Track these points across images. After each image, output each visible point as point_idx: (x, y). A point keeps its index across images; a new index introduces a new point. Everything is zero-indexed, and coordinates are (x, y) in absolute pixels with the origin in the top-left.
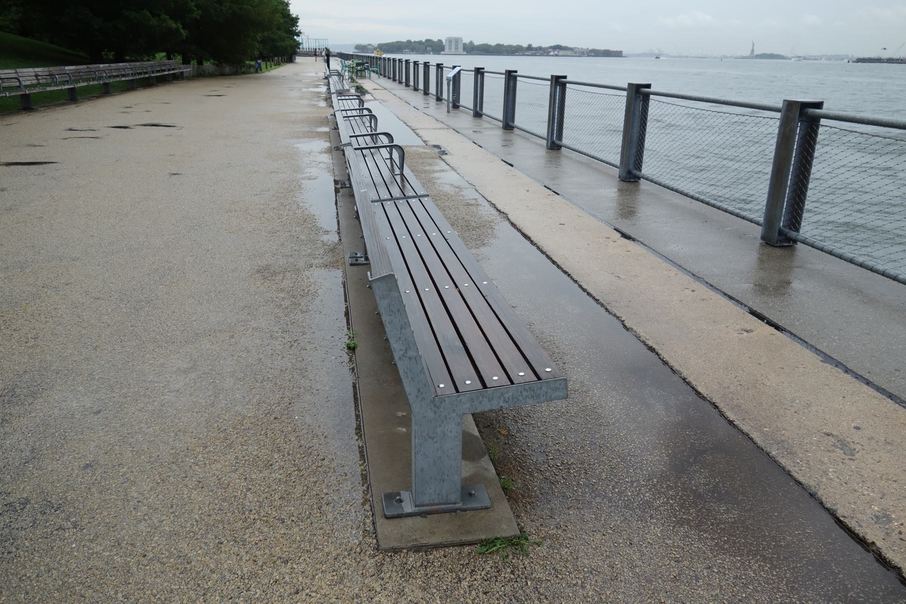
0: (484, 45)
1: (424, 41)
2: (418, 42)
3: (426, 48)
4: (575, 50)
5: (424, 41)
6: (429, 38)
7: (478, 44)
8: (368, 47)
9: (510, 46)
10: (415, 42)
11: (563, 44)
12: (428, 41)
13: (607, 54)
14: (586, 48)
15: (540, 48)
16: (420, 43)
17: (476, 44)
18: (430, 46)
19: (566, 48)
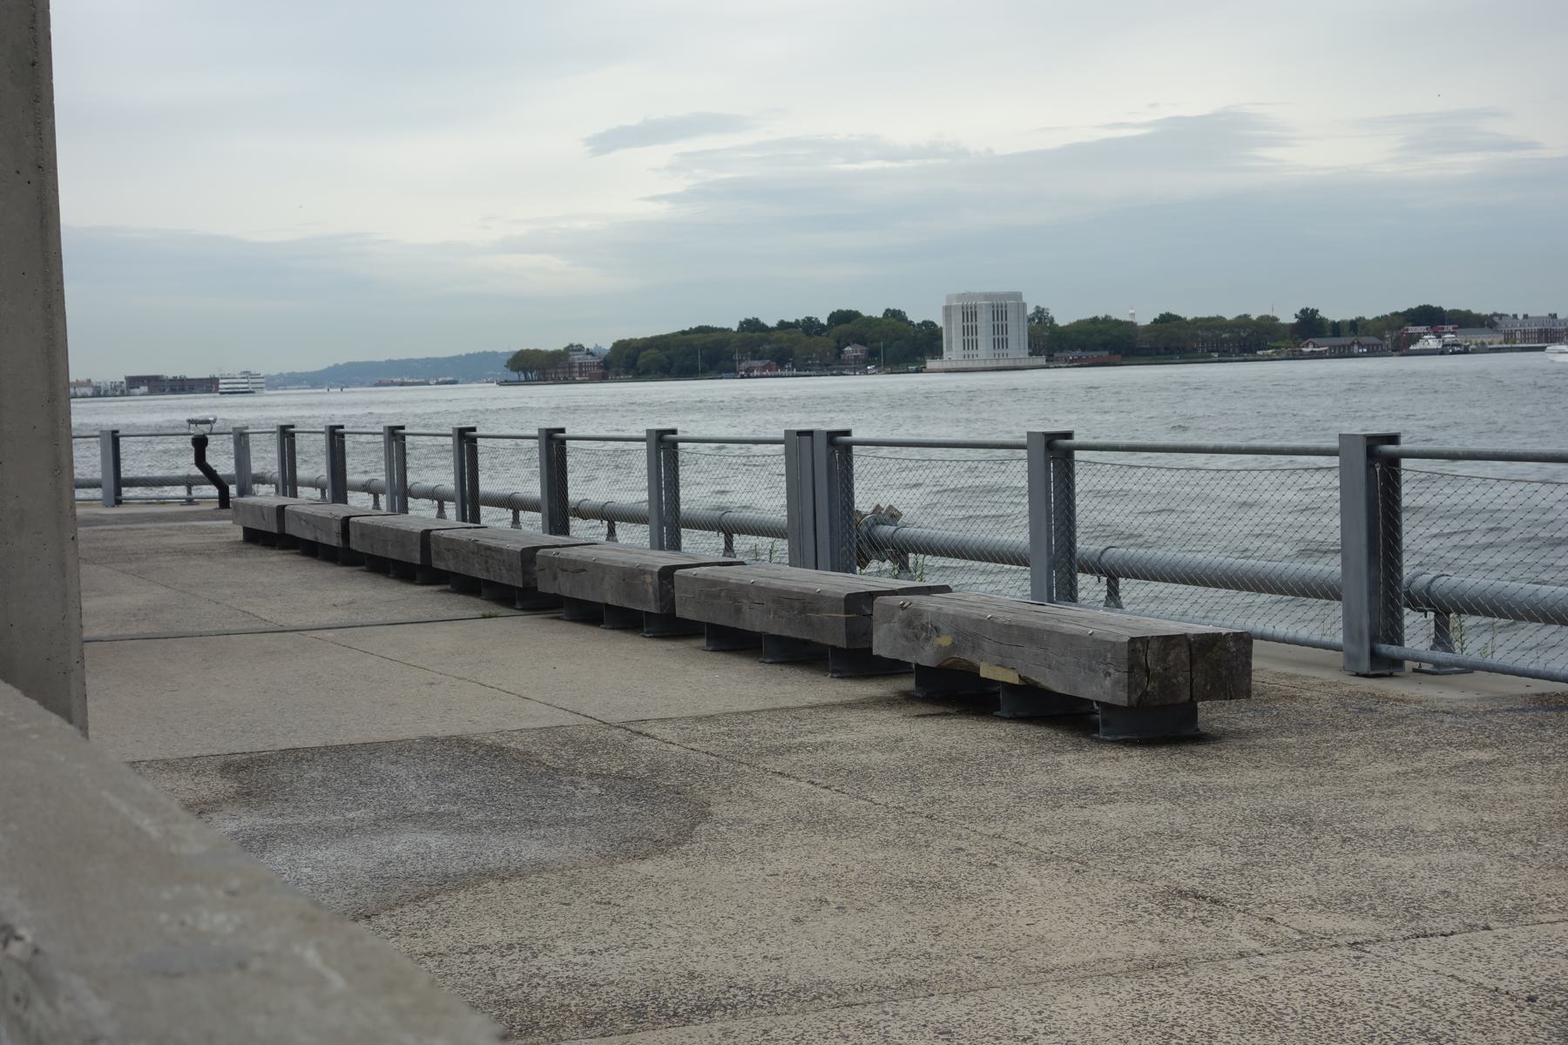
0: (1095, 320)
1: (824, 321)
2: (796, 324)
3: (840, 351)
4: (1504, 326)
5: (824, 321)
7: (1066, 324)
8: (577, 358)
9: (1213, 325)
10: (783, 325)
12: (840, 318)
14: (1544, 312)
15: (1356, 326)
16: (810, 326)
17: (1062, 320)
18: (860, 340)
19: (1465, 320)
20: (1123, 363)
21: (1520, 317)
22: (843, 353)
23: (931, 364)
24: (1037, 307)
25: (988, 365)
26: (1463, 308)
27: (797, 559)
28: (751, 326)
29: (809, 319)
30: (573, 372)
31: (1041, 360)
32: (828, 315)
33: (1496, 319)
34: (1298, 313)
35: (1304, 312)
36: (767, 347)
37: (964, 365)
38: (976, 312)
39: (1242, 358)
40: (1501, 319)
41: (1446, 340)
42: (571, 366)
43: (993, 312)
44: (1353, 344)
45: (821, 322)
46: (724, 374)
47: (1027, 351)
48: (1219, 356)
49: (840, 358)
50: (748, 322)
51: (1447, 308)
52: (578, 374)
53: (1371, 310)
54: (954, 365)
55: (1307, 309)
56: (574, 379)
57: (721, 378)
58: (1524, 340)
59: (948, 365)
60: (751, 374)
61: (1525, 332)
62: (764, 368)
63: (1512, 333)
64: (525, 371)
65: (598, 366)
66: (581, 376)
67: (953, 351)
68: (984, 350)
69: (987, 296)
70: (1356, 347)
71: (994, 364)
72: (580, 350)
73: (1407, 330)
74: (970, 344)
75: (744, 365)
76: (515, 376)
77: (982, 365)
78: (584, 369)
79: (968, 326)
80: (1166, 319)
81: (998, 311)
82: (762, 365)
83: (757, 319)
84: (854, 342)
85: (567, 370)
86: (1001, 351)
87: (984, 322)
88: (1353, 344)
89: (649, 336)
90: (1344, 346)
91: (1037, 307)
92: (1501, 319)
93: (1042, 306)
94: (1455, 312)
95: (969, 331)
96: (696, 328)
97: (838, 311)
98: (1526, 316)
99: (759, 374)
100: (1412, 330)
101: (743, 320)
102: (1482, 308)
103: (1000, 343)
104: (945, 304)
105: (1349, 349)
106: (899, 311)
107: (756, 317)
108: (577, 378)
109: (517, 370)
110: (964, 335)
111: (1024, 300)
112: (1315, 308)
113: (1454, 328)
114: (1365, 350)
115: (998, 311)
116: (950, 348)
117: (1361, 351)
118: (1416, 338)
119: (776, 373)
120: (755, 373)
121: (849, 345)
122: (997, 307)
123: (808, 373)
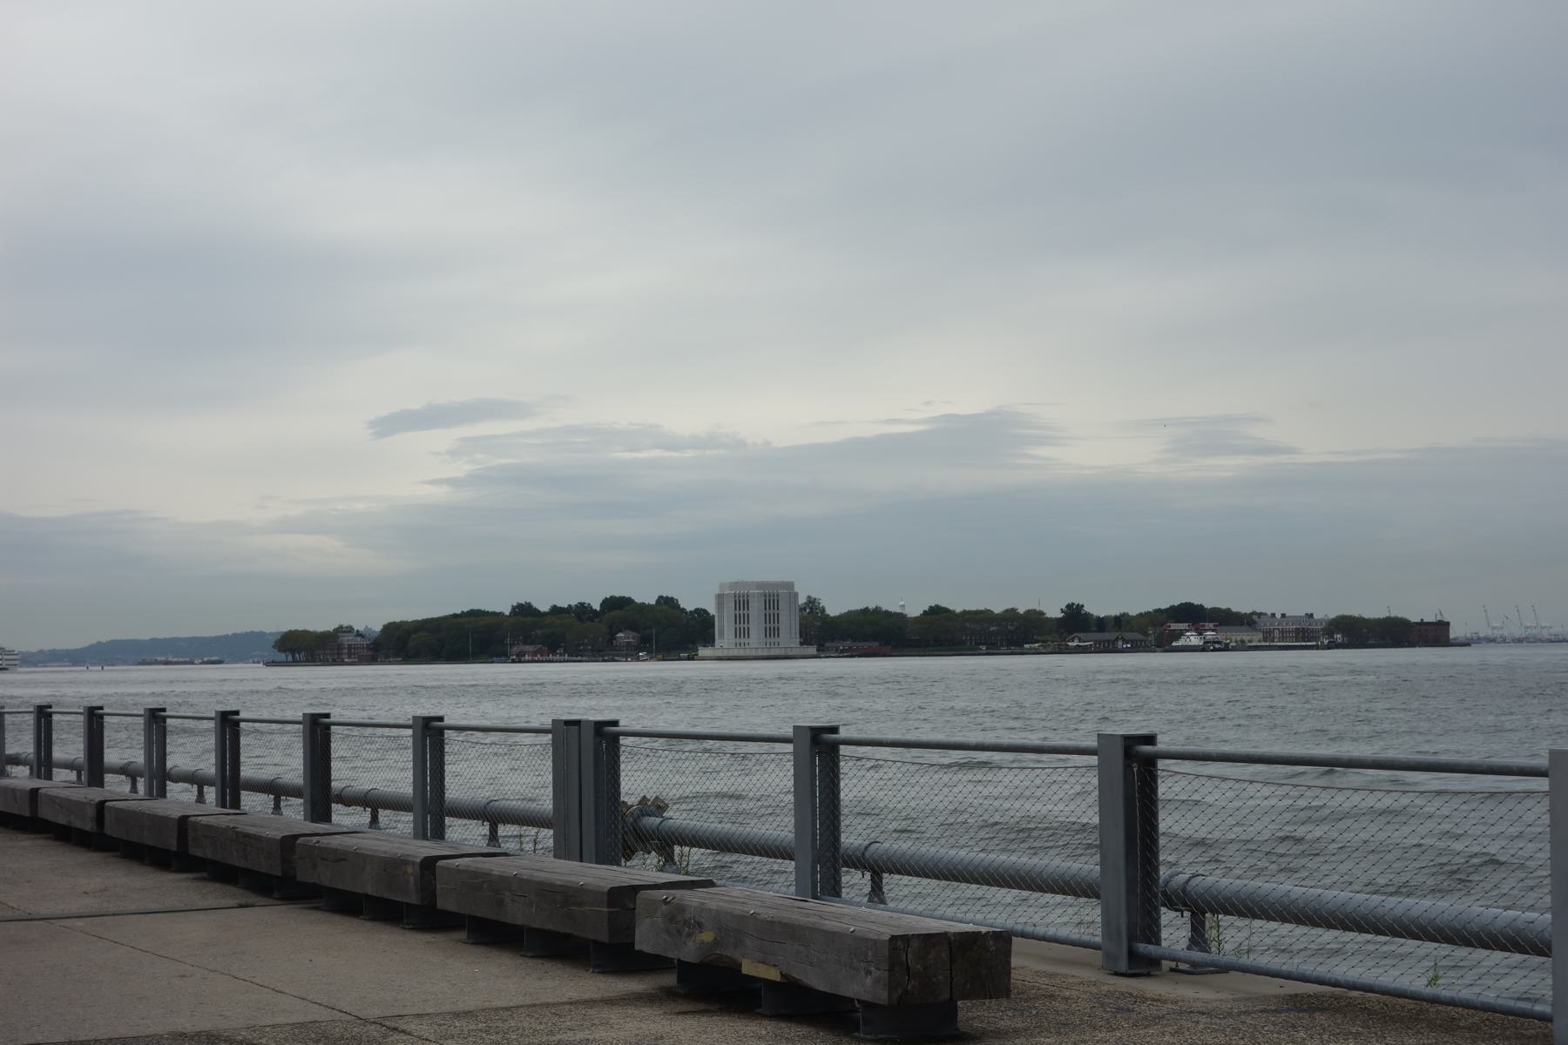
1: (597, 607)
3: (612, 637)
5: (597, 607)
6: (618, 593)
8: (346, 639)
9: (984, 617)
10: (555, 610)
11: (1208, 600)
12: (613, 604)
13: (1395, 633)
14: (1300, 612)
15: (1120, 622)
16: (582, 611)
18: (632, 627)
19: (1225, 618)
20: (893, 654)
21: (1278, 616)
22: (615, 639)
23: (703, 652)
24: (809, 597)
25: (760, 653)
26: (1224, 607)
27: (561, 851)
28: (524, 610)
29: (582, 604)
30: (342, 654)
31: (812, 650)
32: (601, 601)
33: (1255, 617)
34: (1064, 607)
35: (1069, 606)
36: (539, 632)
37: (735, 653)
38: (748, 601)
39: (1009, 651)
40: (1259, 617)
41: (1208, 637)
42: (340, 647)
43: (765, 601)
44: (1117, 639)
45: (594, 608)
46: (495, 659)
47: (798, 640)
48: (987, 649)
49: (612, 643)
50: (520, 606)
51: (1208, 605)
52: (347, 656)
53: (1135, 606)
54: (725, 653)
55: (1073, 604)
56: (343, 660)
57: (492, 662)
58: (1283, 639)
59: (720, 653)
60: (523, 659)
61: (1282, 631)
62: (535, 653)
63: (1270, 632)
64: (293, 651)
65: (368, 647)
66: (349, 657)
67: (725, 640)
68: (756, 639)
69: (760, 585)
70: (1120, 643)
71: (765, 653)
72: (350, 632)
73: (1170, 626)
74: (743, 632)
75: (515, 649)
76: (282, 657)
77: (754, 653)
78: (353, 651)
79: (744, 614)
80: (936, 612)
81: (769, 600)
82: (535, 649)
83: (530, 603)
84: (626, 629)
85: (336, 651)
86: (772, 640)
87: (756, 610)
88: (1117, 639)
89: (420, 618)
90: (1108, 641)
91: (809, 597)
92: (1259, 617)
93: (813, 596)
94: (1216, 610)
95: (741, 619)
96: (468, 612)
97: (611, 597)
98: (1283, 616)
99: (530, 658)
100: (1174, 626)
101: (515, 604)
102: (1242, 607)
103: (772, 632)
104: (717, 592)
105: (1113, 644)
106: (672, 598)
107: (528, 601)
108: (346, 660)
109: (285, 651)
110: (736, 623)
111: (796, 590)
112: (1081, 604)
113: (1214, 626)
114: (1129, 646)
115: (769, 600)
116: (722, 636)
117: (1125, 646)
118: (1179, 635)
119: (548, 658)
120: (527, 658)
121: (621, 631)
122: (770, 596)
123: (579, 658)
